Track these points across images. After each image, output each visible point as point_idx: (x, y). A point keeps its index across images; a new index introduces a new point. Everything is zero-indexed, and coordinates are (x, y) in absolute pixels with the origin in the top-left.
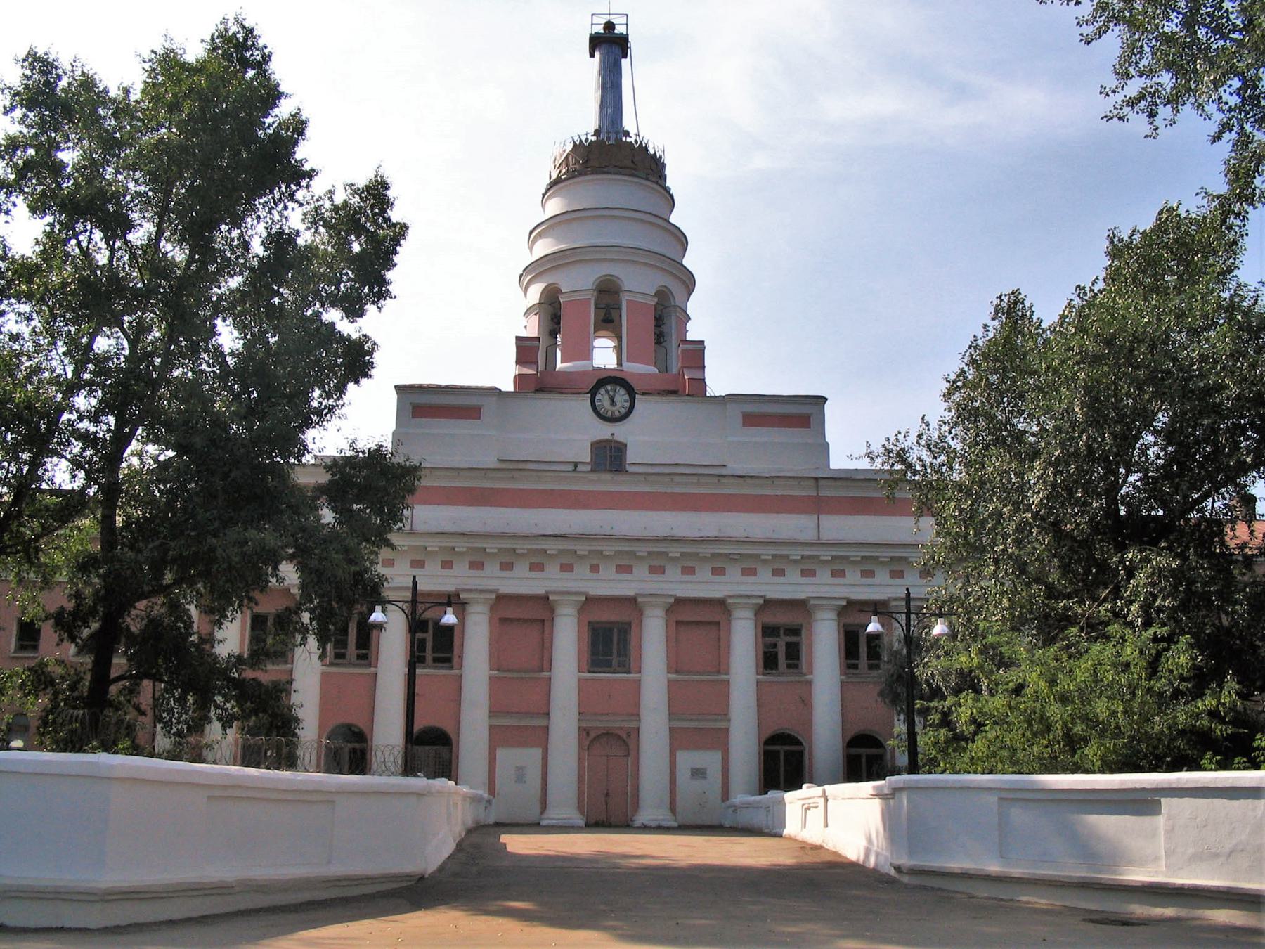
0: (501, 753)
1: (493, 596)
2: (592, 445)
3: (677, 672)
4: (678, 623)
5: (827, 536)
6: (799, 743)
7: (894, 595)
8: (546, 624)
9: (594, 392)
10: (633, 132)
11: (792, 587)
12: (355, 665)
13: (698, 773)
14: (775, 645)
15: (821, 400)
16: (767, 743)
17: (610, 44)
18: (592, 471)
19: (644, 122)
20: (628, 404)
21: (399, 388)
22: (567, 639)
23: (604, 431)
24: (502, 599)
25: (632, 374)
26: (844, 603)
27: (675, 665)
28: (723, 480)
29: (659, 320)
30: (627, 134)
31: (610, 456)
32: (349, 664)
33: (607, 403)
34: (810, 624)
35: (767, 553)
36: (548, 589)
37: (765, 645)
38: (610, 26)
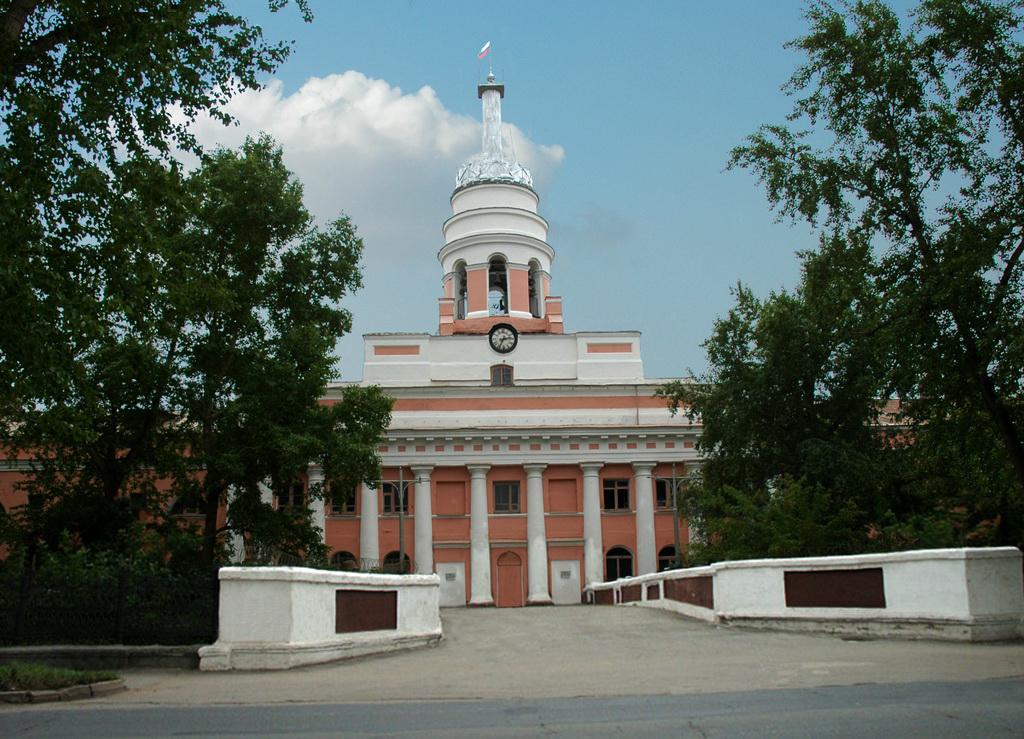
2: (491, 368)
3: (550, 511)
4: (550, 481)
5: (642, 423)
6: (629, 554)
7: (687, 459)
9: (491, 333)
11: (622, 455)
16: (608, 554)
22: (480, 492)
23: (499, 359)
27: (549, 505)
28: (576, 389)
29: (532, 282)
31: (503, 375)
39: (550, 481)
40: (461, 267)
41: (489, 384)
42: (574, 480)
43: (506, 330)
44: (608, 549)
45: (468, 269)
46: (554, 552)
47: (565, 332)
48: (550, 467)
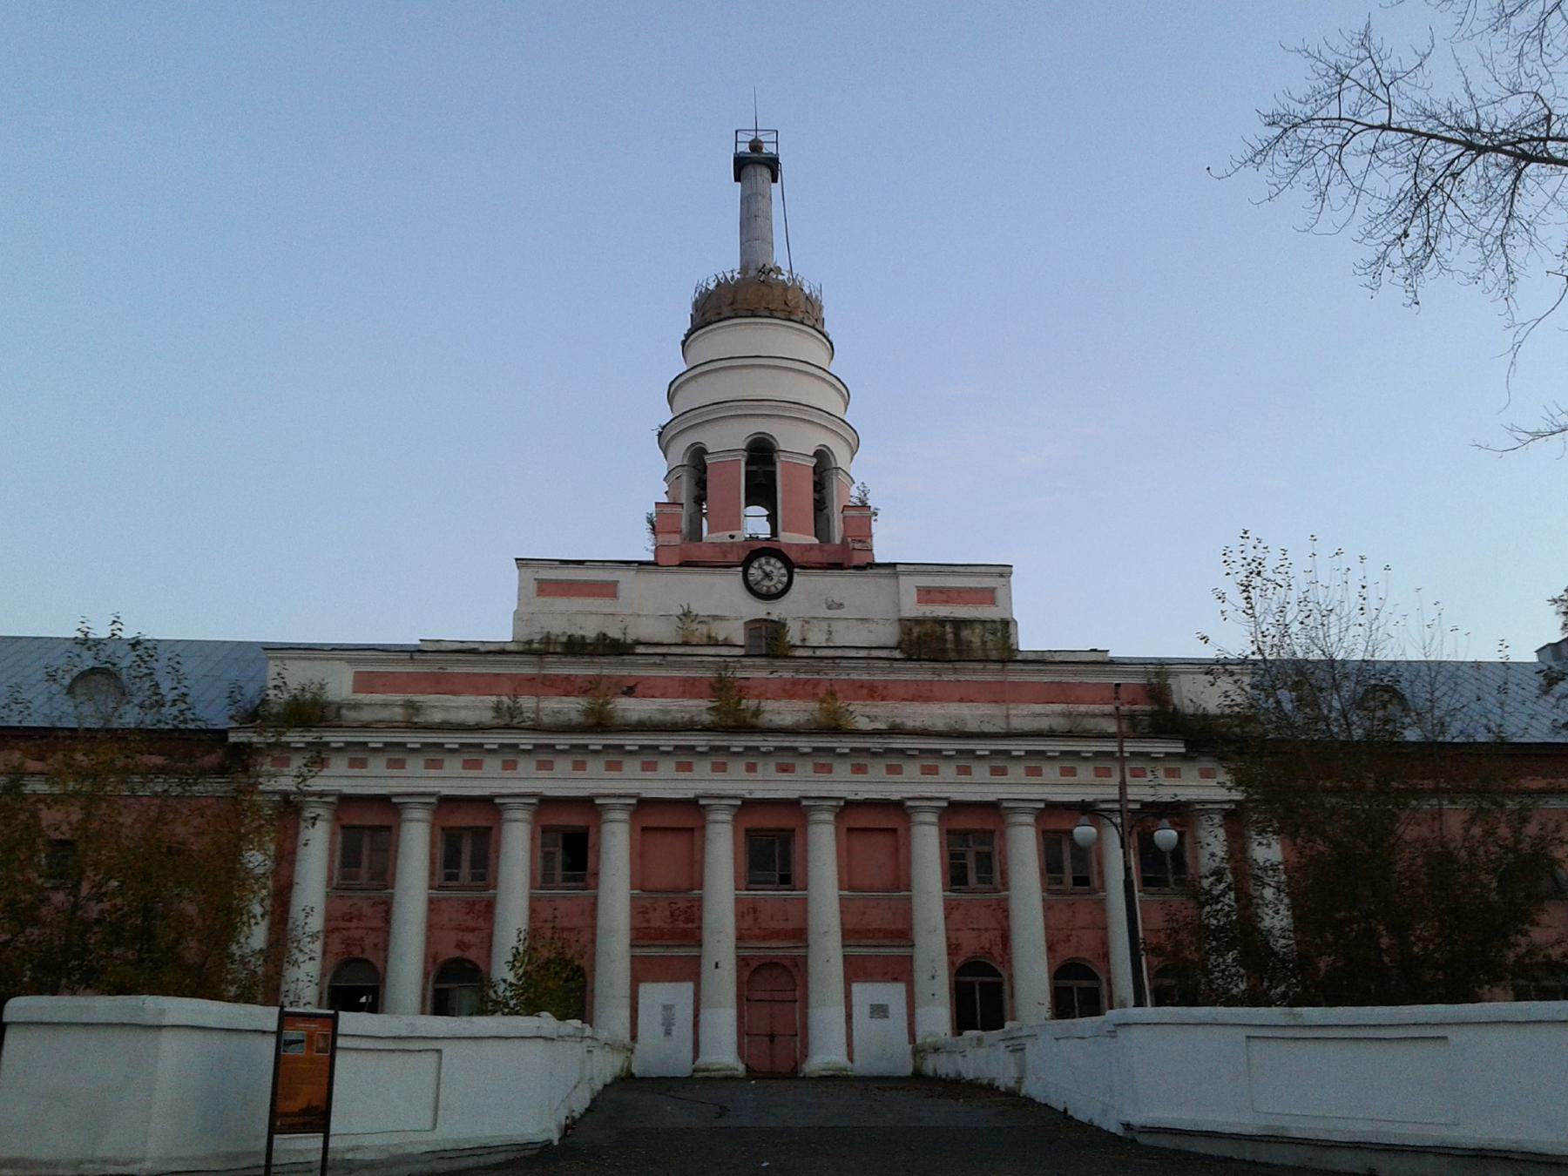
1: (634, 801)
3: (850, 888)
5: (1018, 724)
8: (696, 834)
9: (746, 564)
10: (785, 268)
11: (979, 787)
12: (471, 889)
13: (879, 1011)
14: (963, 856)
15: (1004, 571)
17: (755, 164)
19: (798, 256)
21: (520, 561)
22: (722, 848)
23: (759, 610)
24: (644, 805)
25: (789, 546)
26: (1042, 805)
27: (847, 882)
30: (779, 271)
31: (769, 640)
34: (1003, 834)
35: (949, 746)
36: (698, 792)
37: (953, 856)
38: (756, 146)
39: (850, 830)
40: (698, 455)
41: (742, 652)
42: (894, 830)
43: (773, 561)
44: (960, 961)
45: (709, 460)
46: (856, 970)
47: (877, 560)
48: (850, 804)
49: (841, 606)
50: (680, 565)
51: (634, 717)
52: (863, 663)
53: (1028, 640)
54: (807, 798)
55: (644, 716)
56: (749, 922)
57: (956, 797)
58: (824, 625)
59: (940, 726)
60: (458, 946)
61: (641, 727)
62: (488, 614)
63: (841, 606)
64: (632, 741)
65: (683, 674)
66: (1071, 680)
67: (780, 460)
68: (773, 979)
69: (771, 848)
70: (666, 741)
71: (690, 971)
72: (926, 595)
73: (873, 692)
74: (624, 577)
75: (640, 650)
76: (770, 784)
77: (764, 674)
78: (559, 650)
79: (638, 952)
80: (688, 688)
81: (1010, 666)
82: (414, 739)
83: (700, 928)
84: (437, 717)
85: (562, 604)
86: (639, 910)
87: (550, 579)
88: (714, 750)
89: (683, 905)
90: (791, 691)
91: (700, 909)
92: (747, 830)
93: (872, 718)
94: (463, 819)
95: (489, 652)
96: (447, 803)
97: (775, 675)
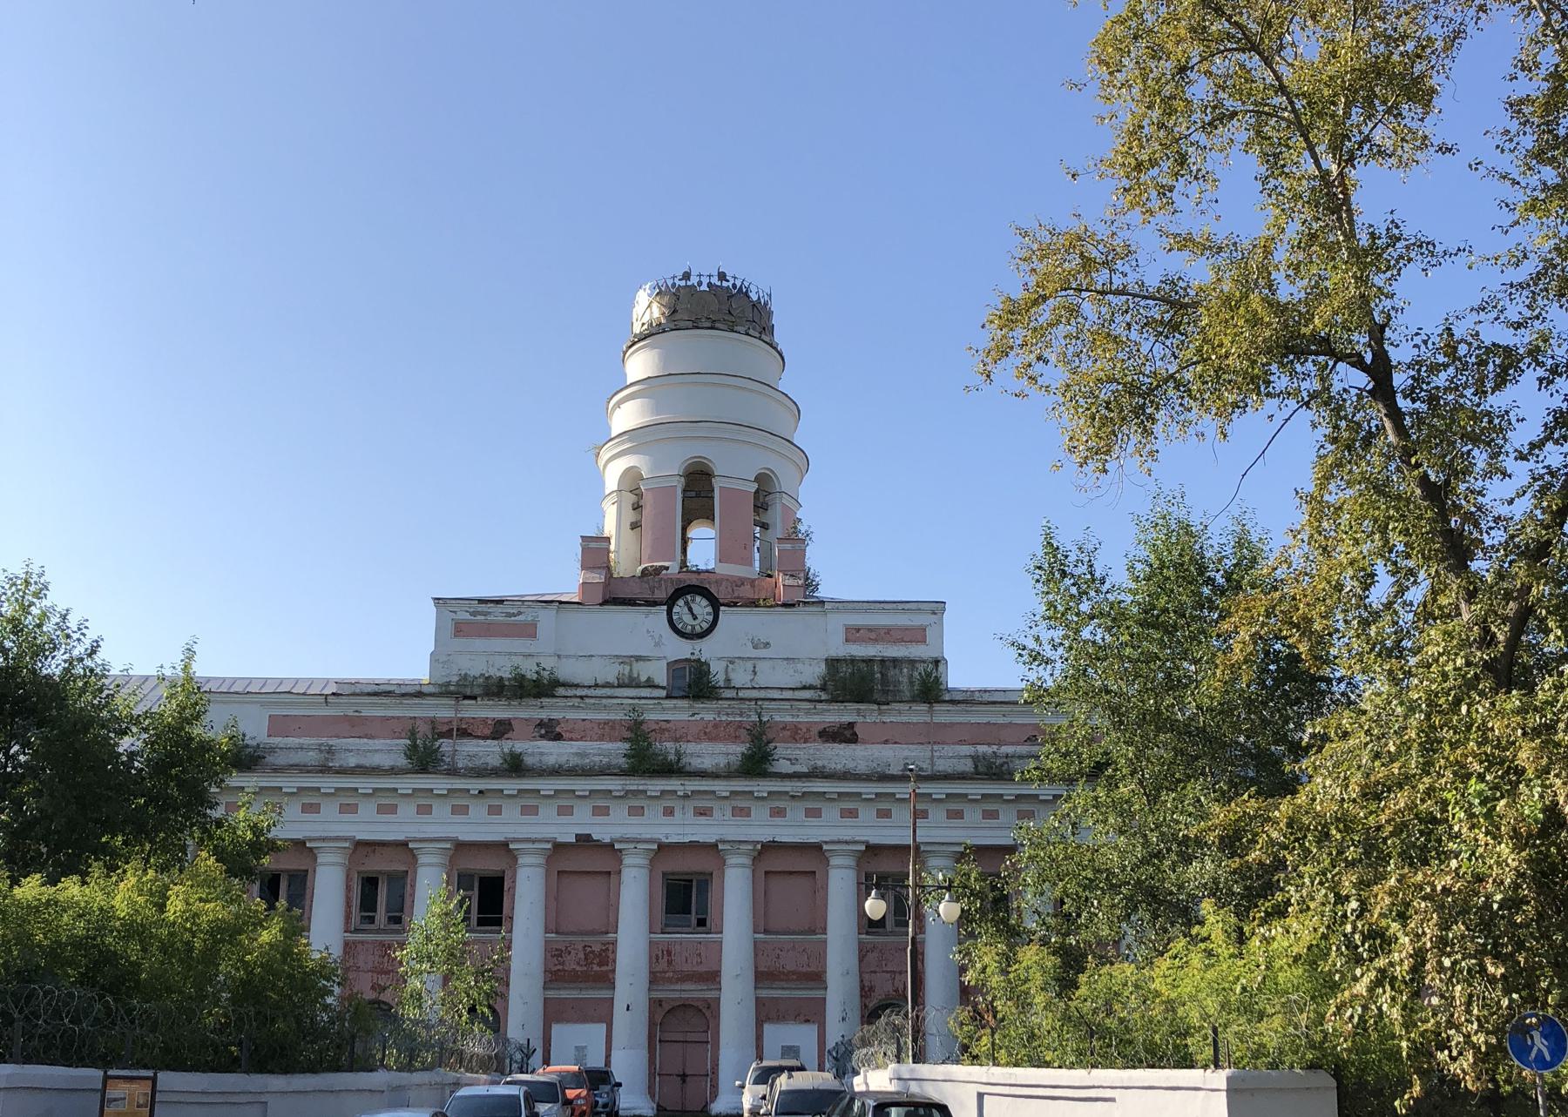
0: (556, 1029)
1: (549, 846)
3: (766, 932)
5: (943, 766)
9: (670, 603)
12: (385, 931)
15: (937, 608)
18: (668, 697)
20: (711, 618)
21: (438, 601)
22: (635, 895)
23: (683, 650)
32: (378, 931)
33: (687, 618)
43: (698, 598)
46: (765, 1013)
49: (767, 645)
50: (605, 603)
51: (551, 761)
52: (787, 705)
53: (957, 678)
54: (725, 842)
55: (562, 760)
56: (663, 965)
57: (874, 840)
58: (749, 665)
59: (862, 768)
60: (373, 988)
61: (556, 772)
62: (404, 654)
63: (767, 645)
64: (547, 785)
65: (603, 716)
66: (1001, 720)
67: (717, 484)
68: (681, 1023)
69: (684, 896)
70: (582, 785)
71: (603, 1013)
72: (853, 634)
73: (796, 734)
74: (546, 618)
75: (561, 691)
76: (684, 828)
77: (685, 716)
78: (477, 691)
79: (552, 994)
80: (606, 730)
81: (937, 707)
82: (328, 783)
83: (614, 971)
84: (352, 761)
85: (479, 644)
86: (554, 954)
87: (468, 619)
88: (628, 794)
89: (597, 948)
90: (711, 733)
91: (614, 952)
92: (664, 874)
93: (793, 761)
94: (376, 864)
95: (403, 695)
96: (363, 847)
97: (697, 717)
